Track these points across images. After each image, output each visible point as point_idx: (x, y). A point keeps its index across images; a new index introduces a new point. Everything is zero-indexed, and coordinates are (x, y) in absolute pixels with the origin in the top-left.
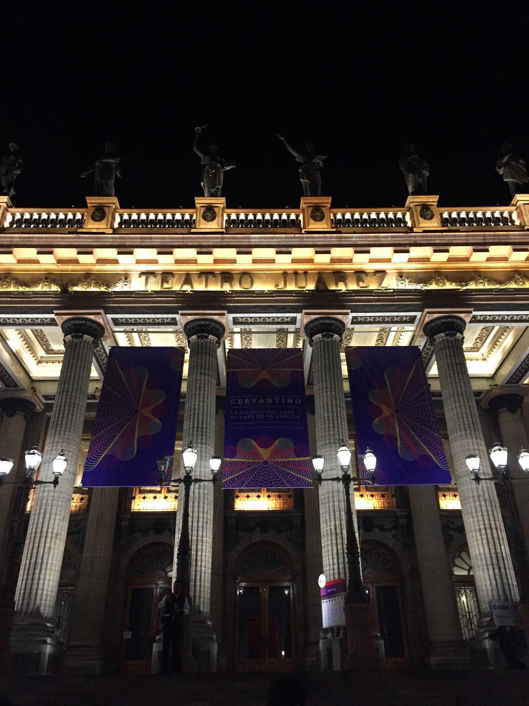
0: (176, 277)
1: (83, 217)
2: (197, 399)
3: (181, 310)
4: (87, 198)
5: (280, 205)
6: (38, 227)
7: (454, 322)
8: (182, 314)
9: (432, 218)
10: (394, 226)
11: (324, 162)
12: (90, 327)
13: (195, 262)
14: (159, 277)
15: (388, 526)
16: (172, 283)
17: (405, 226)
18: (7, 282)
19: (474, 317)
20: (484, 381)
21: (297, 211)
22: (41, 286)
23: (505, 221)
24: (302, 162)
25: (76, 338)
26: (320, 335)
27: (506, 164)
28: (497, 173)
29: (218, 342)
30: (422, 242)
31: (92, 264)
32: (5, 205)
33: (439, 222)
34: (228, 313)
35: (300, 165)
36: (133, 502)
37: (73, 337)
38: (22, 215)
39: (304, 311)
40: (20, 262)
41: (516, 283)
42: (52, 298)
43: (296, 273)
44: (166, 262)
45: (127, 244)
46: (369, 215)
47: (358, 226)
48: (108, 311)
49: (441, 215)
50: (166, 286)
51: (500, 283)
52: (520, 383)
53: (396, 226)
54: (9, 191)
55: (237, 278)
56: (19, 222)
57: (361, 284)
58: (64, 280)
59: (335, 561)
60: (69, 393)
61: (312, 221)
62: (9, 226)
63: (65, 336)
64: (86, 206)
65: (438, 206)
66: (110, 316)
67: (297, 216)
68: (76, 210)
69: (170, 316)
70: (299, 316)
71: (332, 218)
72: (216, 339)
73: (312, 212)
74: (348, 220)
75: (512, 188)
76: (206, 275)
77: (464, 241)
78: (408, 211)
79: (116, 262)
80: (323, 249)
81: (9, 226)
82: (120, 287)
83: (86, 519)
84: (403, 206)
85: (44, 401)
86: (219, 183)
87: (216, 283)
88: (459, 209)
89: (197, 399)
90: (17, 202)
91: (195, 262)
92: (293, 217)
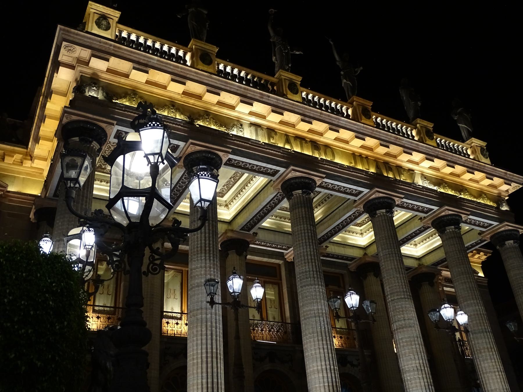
15: (355, 362)
26: (384, 211)
30: (441, 157)
42: (182, 126)
43: (360, 155)
45: (249, 95)
51: (475, 197)
55: (322, 148)
77: (462, 163)
82: (234, 132)
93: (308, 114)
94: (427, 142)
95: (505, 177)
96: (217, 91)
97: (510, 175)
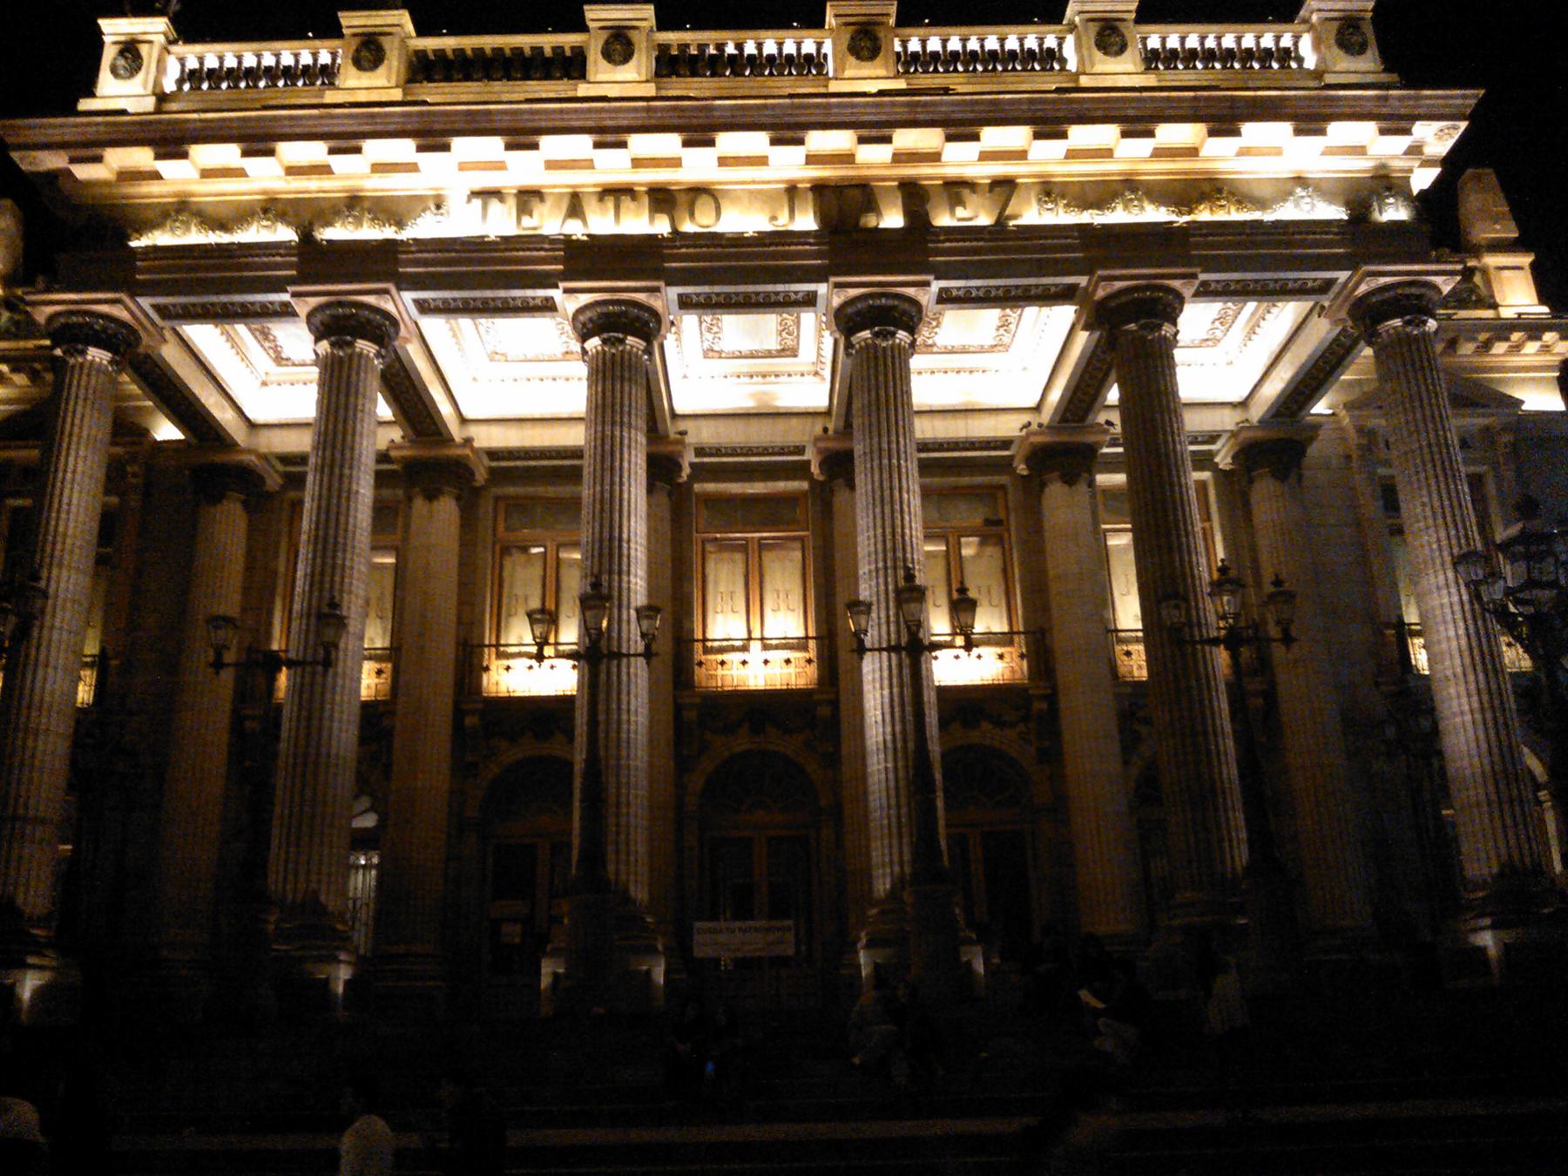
0: (549, 202)
1: (334, 60)
2: (607, 480)
3: (565, 279)
4: (340, 14)
5: (779, 21)
6: (237, 87)
8: (566, 291)
9: (1122, 49)
10: (1037, 67)
13: (589, 164)
14: (512, 203)
16: (542, 215)
17: (1063, 69)
18: (182, 222)
19: (1204, 284)
20: (1227, 412)
21: (816, 32)
22: (254, 227)
23: (1285, 55)
25: (341, 347)
26: (866, 334)
29: (649, 351)
31: (362, 177)
32: (162, 38)
33: (1138, 58)
34: (668, 284)
36: (485, 677)
37: (332, 345)
38: (201, 60)
39: (833, 279)
40: (207, 174)
41: (1297, 205)
44: (524, 168)
45: (437, 127)
47: (956, 70)
49: (1144, 40)
50: (527, 221)
53: (1043, 69)
55: (682, 199)
56: (194, 76)
57: (960, 212)
59: (893, 801)
61: (852, 60)
63: (317, 340)
64: (340, 35)
65: (1138, 21)
66: (408, 296)
67: (819, 45)
68: (318, 43)
69: (542, 293)
70: (822, 289)
71: (898, 48)
72: (641, 344)
74: (935, 55)
76: (616, 193)
78: (1071, 32)
79: (412, 168)
80: (874, 133)
82: (425, 228)
83: (392, 713)
84: (1060, 22)
85: (281, 468)
88: (1183, 28)
89: (607, 480)
90: (189, 30)
91: (589, 164)
92: (809, 47)
93: (609, 123)
94: (1098, 68)
95: (1385, 111)
96: (353, 143)
97: (1400, 98)
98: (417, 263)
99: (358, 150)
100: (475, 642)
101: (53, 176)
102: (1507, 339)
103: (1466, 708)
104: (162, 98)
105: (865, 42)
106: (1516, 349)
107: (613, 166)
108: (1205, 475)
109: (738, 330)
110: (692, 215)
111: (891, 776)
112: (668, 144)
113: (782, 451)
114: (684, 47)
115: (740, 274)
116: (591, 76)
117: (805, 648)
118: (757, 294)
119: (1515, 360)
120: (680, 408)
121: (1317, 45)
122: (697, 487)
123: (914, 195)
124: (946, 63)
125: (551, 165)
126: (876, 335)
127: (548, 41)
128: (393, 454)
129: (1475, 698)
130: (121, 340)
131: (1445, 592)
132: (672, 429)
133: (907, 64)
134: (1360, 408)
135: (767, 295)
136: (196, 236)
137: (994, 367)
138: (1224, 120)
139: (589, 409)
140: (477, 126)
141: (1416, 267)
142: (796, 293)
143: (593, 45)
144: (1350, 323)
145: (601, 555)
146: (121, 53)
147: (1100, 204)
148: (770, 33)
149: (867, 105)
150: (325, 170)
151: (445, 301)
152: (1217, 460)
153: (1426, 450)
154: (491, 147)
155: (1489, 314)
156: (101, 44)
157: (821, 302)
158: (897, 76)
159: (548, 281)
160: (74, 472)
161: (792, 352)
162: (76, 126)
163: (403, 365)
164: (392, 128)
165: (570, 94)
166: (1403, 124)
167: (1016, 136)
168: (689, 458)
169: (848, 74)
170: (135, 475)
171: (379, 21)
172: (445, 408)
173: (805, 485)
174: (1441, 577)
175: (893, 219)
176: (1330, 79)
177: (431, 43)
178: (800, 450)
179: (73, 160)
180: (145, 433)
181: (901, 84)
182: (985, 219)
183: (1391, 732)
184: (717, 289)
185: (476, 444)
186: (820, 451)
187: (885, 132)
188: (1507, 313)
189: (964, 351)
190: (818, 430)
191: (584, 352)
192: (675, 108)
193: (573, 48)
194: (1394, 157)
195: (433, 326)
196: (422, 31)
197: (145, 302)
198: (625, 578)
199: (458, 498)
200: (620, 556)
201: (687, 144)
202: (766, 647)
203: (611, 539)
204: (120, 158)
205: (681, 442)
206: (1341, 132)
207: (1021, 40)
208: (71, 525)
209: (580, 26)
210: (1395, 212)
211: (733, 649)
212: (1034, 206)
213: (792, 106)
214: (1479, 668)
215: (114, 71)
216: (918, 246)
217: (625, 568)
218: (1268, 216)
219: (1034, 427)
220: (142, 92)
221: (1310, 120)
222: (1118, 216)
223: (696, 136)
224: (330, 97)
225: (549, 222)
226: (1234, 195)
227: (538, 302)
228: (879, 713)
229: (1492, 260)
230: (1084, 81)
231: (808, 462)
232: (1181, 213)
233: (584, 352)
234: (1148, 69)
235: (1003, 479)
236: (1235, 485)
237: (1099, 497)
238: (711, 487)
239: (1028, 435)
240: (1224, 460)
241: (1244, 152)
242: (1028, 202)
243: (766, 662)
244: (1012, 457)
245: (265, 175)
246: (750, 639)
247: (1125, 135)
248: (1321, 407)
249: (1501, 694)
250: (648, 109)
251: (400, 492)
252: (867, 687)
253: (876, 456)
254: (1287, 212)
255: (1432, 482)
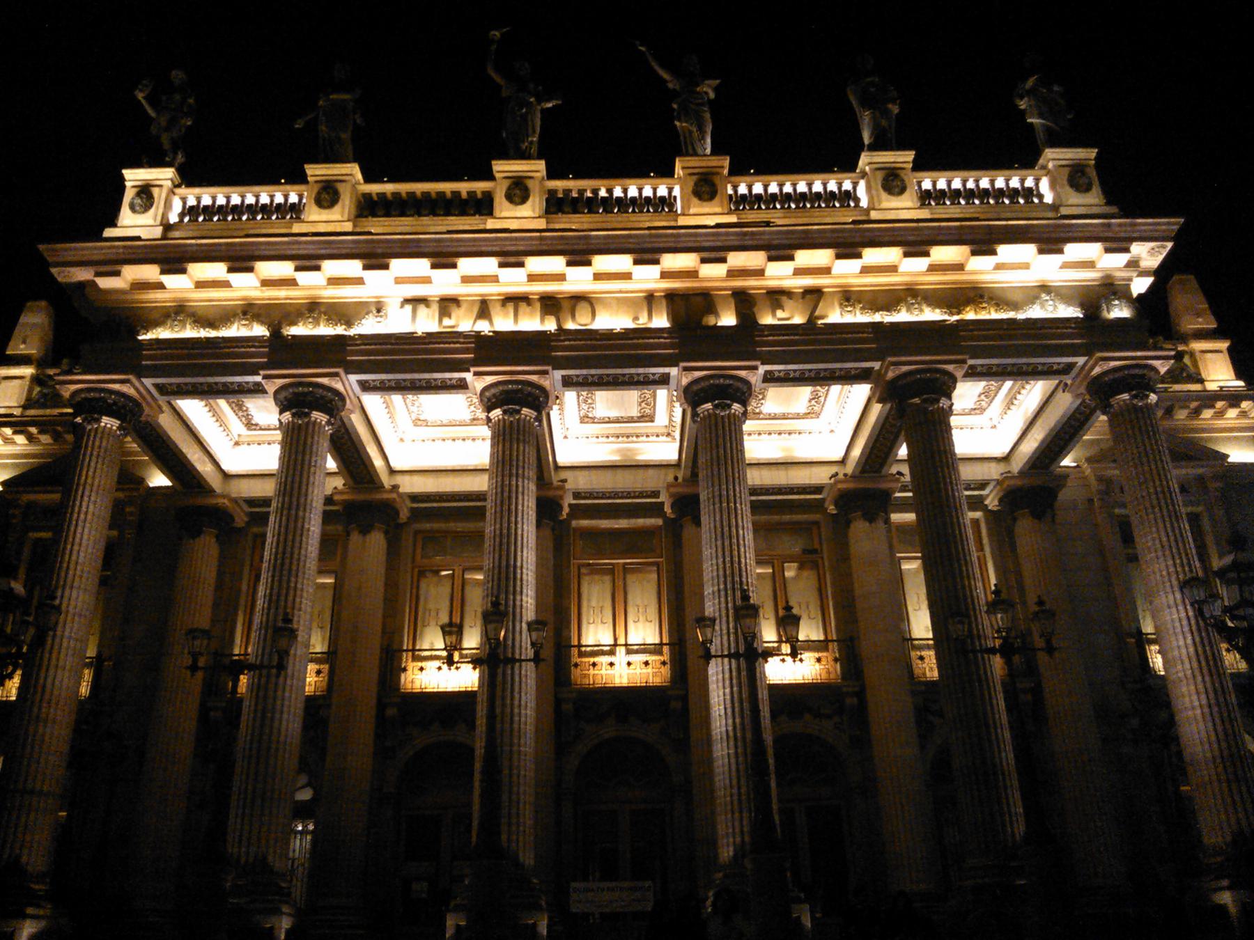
0: (464, 306)
1: (300, 200)
3: (474, 366)
5: (639, 172)
6: (225, 220)
7: (937, 379)
8: (476, 374)
9: (902, 190)
10: (837, 205)
11: (716, 89)
12: (322, 397)
13: (495, 279)
14: (435, 308)
16: (458, 317)
17: (857, 205)
19: (971, 367)
20: (993, 465)
21: (669, 181)
22: (235, 326)
23: (1028, 193)
24: (678, 87)
26: (709, 406)
27: (1031, 93)
28: (1017, 106)
31: (320, 288)
32: (169, 183)
33: (916, 199)
35: (674, 94)
36: (403, 676)
37: (293, 415)
38: (199, 199)
39: (683, 364)
40: (200, 285)
41: (1043, 306)
44: (445, 282)
45: (379, 251)
46: (794, 185)
47: (775, 207)
48: (352, 368)
49: (919, 183)
50: (446, 322)
52: (1053, 467)
54: (176, 154)
55: (566, 305)
56: (192, 211)
57: (780, 314)
58: (275, 315)
59: (735, 782)
60: (293, 512)
61: (695, 200)
62: (177, 220)
63: (281, 412)
66: (353, 378)
67: (670, 190)
68: (288, 187)
70: (674, 371)
71: (730, 191)
72: (534, 414)
73: (696, 184)
75: (1041, 136)
76: (515, 301)
79: (359, 281)
81: (177, 220)
82: (368, 326)
83: (329, 706)
86: (534, 132)
87: (532, 314)
90: (189, 177)
91: (495, 279)
92: (662, 191)
94: (885, 205)
95: (1110, 234)
96: (313, 263)
97: (1120, 225)
98: (362, 353)
99: (318, 268)
100: (395, 647)
101: (82, 286)
102: (1213, 407)
103: (1197, 703)
104: (167, 227)
105: (705, 188)
106: (1220, 414)
107: (514, 280)
108: (978, 515)
109: (606, 402)
110: (573, 317)
111: (733, 760)
112: (556, 264)
113: (641, 495)
114: (567, 192)
115: (610, 361)
116: (497, 213)
117: (660, 653)
118: (624, 375)
119: (1220, 423)
120: (562, 459)
121: (1053, 186)
122: (574, 523)
123: (744, 301)
124: (767, 203)
125: (466, 280)
126: (716, 407)
127: (464, 187)
128: (336, 498)
129: (1203, 696)
130: (127, 411)
131: (1174, 610)
132: (555, 478)
133: (737, 203)
134: (1098, 462)
135: (631, 375)
136: (190, 332)
137: (809, 430)
138: (984, 243)
139: (492, 463)
140: (410, 250)
141: (1139, 354)
142: (654, 374)
143: (499, 190)
144: (1087, 397)
145: (499, 579)
146: (138, 194)
147: (889, 307)
148: (632, 181)
149: (706, 235)
150: (292, 283)
151: (382, 382)
152: (986, 502)
153: (1154, 497)
154: (421, 266)
155: (1197, 387)
156: (124, 187)
157: (673, 382)
158: (730, 212)
159: (462, 366)
160: (86, 513)
161: (651, 419)
162: (102, 248)
163: (347, 430)
164: (344, 251)
165: (481, 227)
166: (1124, 245)
167: (821, 257)
168: (568, 500)
169: (692, 211)
170: (131, 514)
171: (336, 172)
172: (378, 463)
173: (659, 522)
174: (1171, 597)
175: (728, 319)
176: (1064, 211)
177: (375, 188)
178: (655, 494)
179: (98, 274)
180: (141, 481)
181: (733, 219)
182: (798, 320)
183: (1135, 722)
184: (593, 372)
185: (401, 490)
186: (671, 495)
187: (722, 254)
188: (1212, 386)
189: (784, 417)
190: (670, 478)
191: (489, 420)
192: (562, 238)
193: (483, 193)
194: (1120, 269)
195: (372, 402)
196: (368, 179)
197: (148, 382)
198: (518, 597)
199: (386, 533)
200: (515, 578)
201: (569, 264)
202: (629, 652)
203: (508, 566)
204: (132, 273)
205: (562, 488)
206: (1074, 251)
207: (825, 185)
208: (82, 554)
209: (490, 177)
210: (1119, 312)
211: (603, 653)
212: (838, 311)
213: (651, 236)
214: (1205, 671)
215: (132, 208)
216: (748, 340)
217: (518, 589)
218: (1021, 316)
219: (841, 476)
220: (151, 222)
221: (1050, 242)
222: (903, 316)
223: (578, 258)
224: (297, 228)
225: (464, 322)
226: (991, 298)
227: (454, 382)
228: (722, 707)
229: (1197, 346)
230: (874, 215)
231: (662, 504)
232: (952, 314)
233: (489, 420)
234: (923, 205)
235: (817, 517)
236: (1002, 522)
237: (894, 529)
238: (585, 523)
239: (836, 482)
240: (992, 502)
241: (999, 267)
242: (833, 308)
243: (629, 664)
244: (823, 500)
245: (245, 286)
246: (615, 645)
247: (906, 255)
248: (1067, 462)
249: (1224, 692)
250: (541, 238)
251: (340, 528)
252: (712, 686)
253: (717, 500)
254: (1035, 312)
255: (1159, 521)
